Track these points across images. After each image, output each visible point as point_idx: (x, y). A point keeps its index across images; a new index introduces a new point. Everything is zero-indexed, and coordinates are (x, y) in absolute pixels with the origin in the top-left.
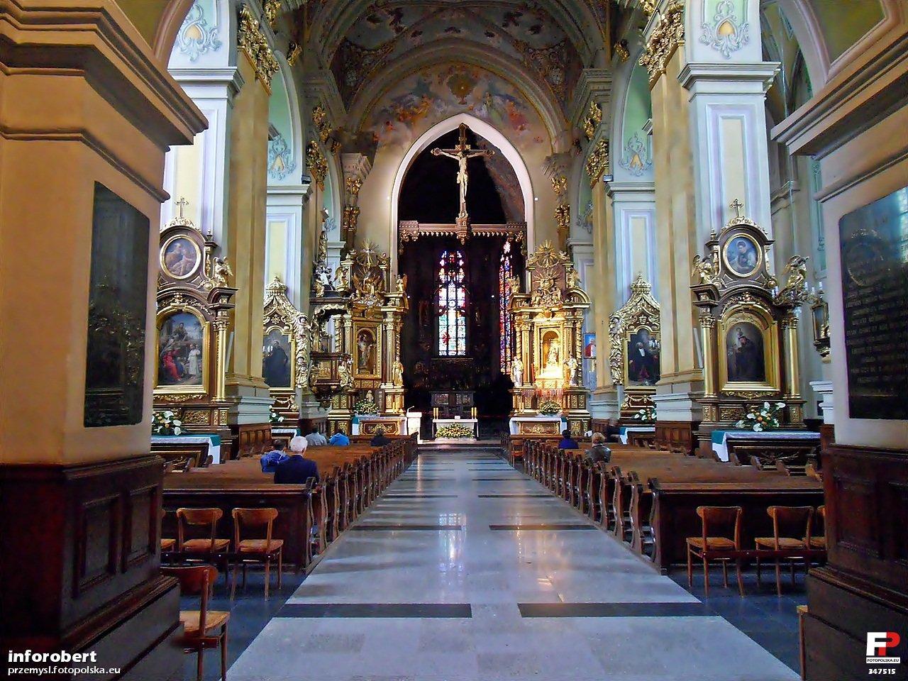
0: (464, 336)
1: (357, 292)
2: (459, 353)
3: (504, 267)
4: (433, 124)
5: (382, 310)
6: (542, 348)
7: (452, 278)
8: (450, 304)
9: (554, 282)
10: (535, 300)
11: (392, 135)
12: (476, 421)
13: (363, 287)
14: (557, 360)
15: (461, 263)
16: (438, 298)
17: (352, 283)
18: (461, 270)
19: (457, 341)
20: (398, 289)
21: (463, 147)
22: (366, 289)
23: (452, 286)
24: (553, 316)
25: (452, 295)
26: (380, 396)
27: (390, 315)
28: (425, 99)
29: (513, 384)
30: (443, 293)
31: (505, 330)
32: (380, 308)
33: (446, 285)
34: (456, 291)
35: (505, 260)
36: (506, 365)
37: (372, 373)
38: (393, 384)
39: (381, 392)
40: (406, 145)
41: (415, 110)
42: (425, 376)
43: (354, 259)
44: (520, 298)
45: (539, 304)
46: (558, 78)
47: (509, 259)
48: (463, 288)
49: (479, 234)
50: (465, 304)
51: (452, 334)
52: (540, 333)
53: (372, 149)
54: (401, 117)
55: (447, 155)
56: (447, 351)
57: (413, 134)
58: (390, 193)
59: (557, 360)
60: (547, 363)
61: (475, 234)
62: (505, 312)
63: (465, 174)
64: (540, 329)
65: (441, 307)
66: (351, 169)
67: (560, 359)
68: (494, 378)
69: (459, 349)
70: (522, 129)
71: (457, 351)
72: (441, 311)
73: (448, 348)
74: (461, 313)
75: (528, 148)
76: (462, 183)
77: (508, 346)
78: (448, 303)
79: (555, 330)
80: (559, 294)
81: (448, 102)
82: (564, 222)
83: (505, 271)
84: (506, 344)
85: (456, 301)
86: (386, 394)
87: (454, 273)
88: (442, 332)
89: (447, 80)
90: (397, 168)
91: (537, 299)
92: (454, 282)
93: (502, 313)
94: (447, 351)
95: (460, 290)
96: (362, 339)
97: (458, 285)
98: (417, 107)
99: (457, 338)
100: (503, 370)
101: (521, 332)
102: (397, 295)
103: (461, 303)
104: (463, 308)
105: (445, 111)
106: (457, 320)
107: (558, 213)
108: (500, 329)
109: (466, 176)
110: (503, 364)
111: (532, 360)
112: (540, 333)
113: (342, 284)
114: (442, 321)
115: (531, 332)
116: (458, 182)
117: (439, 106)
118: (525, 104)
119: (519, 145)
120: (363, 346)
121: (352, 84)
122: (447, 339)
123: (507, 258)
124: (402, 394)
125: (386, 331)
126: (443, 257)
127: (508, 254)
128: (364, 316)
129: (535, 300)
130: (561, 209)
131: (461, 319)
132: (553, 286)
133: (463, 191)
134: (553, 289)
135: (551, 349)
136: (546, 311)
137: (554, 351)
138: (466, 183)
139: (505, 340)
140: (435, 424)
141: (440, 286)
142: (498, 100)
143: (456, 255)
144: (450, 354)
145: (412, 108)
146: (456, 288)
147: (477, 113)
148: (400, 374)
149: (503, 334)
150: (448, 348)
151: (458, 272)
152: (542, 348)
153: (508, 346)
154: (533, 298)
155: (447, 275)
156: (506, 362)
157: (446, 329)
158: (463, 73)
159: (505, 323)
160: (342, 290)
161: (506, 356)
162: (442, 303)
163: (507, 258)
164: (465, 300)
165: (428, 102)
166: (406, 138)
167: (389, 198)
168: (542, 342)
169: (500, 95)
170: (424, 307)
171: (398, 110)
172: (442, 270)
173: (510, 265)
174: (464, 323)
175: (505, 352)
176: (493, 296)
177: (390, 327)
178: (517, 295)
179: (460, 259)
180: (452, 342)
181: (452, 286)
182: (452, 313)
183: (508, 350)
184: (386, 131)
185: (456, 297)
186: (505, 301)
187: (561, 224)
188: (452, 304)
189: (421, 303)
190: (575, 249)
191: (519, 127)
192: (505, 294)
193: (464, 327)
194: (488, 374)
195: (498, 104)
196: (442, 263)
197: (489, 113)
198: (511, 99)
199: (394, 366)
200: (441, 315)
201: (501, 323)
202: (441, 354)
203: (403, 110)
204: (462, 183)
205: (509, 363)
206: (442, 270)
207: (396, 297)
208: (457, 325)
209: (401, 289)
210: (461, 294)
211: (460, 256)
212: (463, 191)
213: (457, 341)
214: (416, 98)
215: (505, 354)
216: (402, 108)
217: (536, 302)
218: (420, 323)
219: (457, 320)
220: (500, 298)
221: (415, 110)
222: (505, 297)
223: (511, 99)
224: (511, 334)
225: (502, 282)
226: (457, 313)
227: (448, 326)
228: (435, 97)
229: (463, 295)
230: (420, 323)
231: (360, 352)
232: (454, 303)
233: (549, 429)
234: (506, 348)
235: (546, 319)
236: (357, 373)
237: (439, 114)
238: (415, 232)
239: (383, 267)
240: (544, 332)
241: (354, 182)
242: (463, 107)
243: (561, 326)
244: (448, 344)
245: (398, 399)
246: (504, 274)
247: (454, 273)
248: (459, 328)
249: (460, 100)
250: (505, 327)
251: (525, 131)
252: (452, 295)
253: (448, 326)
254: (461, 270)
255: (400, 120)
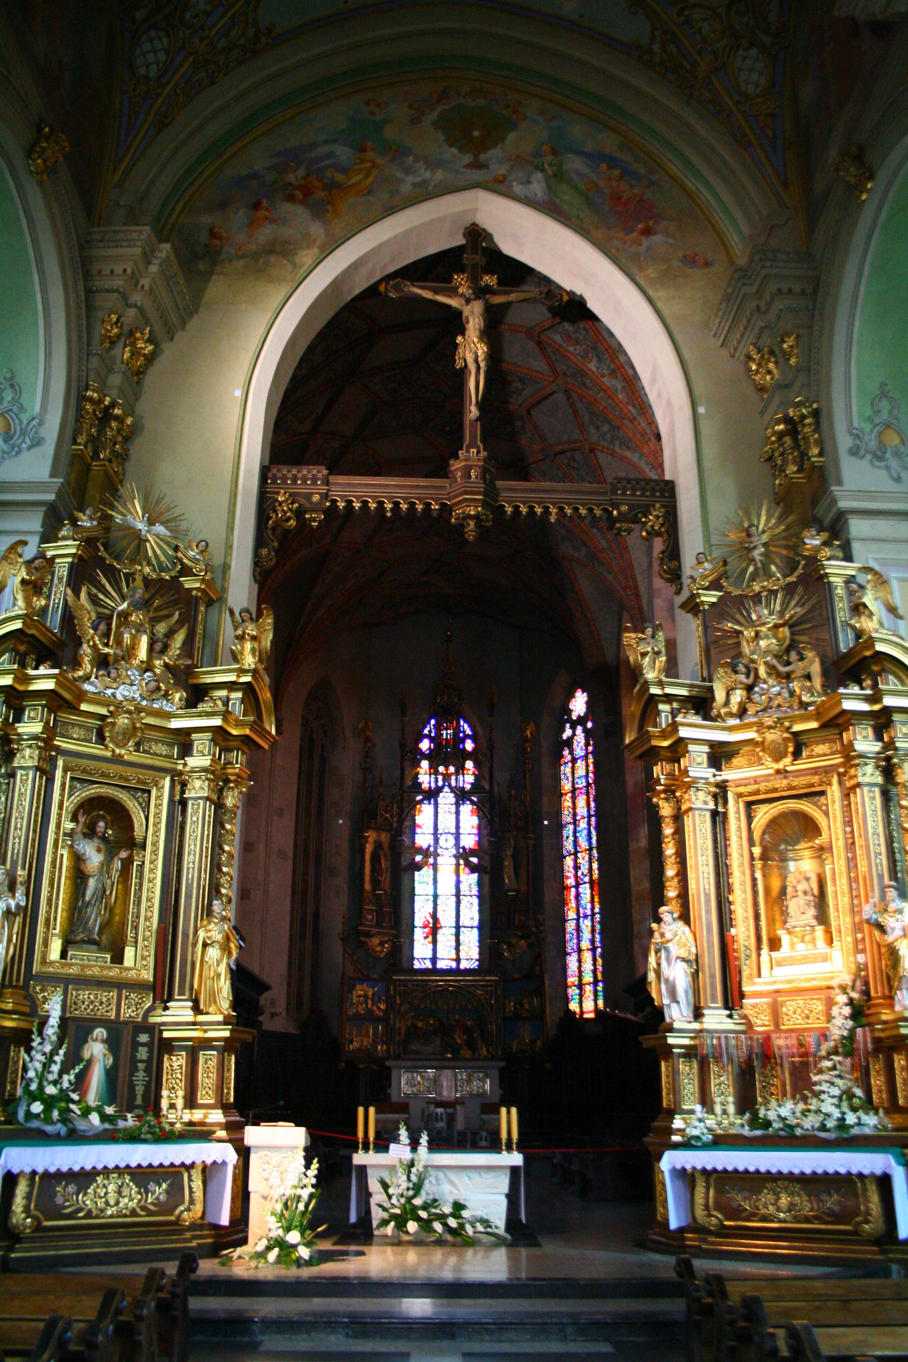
0: (476, 923)
1: (86, 649)
2: (464, 965)
3: (571, 753)
4: (388, 211)
5: (175, 724)
6: (758, 875)
7: (447, 777)
8: (442, 842)
9: (792, 634)
10: (727, 703)
11: (264, 234)
12: (516, 1159)
13: (107, 635)
14: (822, 918)
15: (469, 745)
16: (414, 826)
17: (69, 618)
18: (469, 764)
19: (457, 935)
20: (235, 657)
21: (474, 280)
22: (119, 642)
23: (447, 799)
24: (797, 755)
25: (447, 822)
26: (143, 1053)
27: (201, 742)
28: (370, 155)
29: (658, 1013)
30: (424, 815)
31: (578, 905)
32: (169, 716)
33: (432, 795)
34: (458, 813)
35: (574, 734)
36: (581, 996)
37: (118, 958)
38: (197, 1010)
39: (144, 1038)
40: (306, 257)
41: (339, 177)
42: (375, 1020)
43: (89, 543)
44: (669, 698)
45: (742, 712)
46: (754, 77)
47: (586, 731)
48: (472, 803)
49: (524, 510)
50: (479, 843)
51: (447, 917)
52: (750, 819)
53: (201, 266)
54: (298, 193)
55: (427, 294)
56: (434, 960)
57: (326, 230)
58: (242, 378)
59: (822, 918)
60: (781, 933)
61: (509, 510)
62: (576, 858)
63: (481, 339)
64: (749, 805)
65: (420, 850)
66: (118, 283)
67: (840, 918)
68: (552, 1032)
69: (462, 955)
70: (647, 232)
71: (458, 960)
72: (418, 858)
73: (435, 951)
74: (468, 864)
75: (667, 277)
76: (472, 367)
77: (585, 944)
78: (436, 840)
79: (804, 806)
80: (816, 668)
81: (433, 164)
82: (804, 455)
83: (574, 760)
84: (579, 939)
85: (457, 836)
86: (168, 1047)
87: (452, 769)
88: (422, 911)
89: (434, 116)
90: (269, 315)
91: (738, 696)
92: (452, 790)
93: (569, 862)
94: (434, 960)
95: (466, 809)
96: (90, 833)
97: (461, 796)
98: (345, 171)
99: (458, 927)
100: (574, 1006)
101: (678, 818)
102: (232, 678)
103: (469, 841)
104: (472, 852)
105: (425, 183)
106: (458, 882)
107: (781, 435)
108: (564, 903)
109: (482, 350)
110: (573, 992)
111: (725, 919)
112: (750, 819)
113: (21, 603)
114: (422, 880)
115: (718, 818)
116: (459, 364)
117: (408, 171)
118: (656, 177)
119: (641, 269)
120: (94, 857)
121: (153, 71)
122: (434, 929)
123: (579, 729)
124: (228, 1046)
125: (183, 803)
126: (426, 731)
127: (581, 721)
128: (101, 739)
129: (727, 703)
130: (787, 420)
131: (470, 881)
132: (788, 651)
133: (474, 385)
134: (793, 656)
135: (791, 880)
136: (771, 736)
137: (802, 887)
138: (482, 365)
139: (578, 929)
140: (363, 1169)
141: (419, 798)
142: (574, 164)
143: (457, 730)
144: (440, 965)
145: (328, 174)
146: (457, 805)
147: (518, 189)
148: (223, 969)
149: (572, 915)
150: (435, 951)
151: (461, 769)
152: (758, 875)
153: (585, 944)
154: (720, 695)
155: (436, 773)
156: (580, 986)
157: (431, 905)
158: (481, 102)
159: (577, 885)
160: (18, 625)
161: (580, 972)
162: (423, 839)
163: (579, 729)
164: (479, 834)
165: (379, 161)
166: (308, 241)
167: (238, 393)
168: (757, 851)
169: (580, 153)
170: (378, 846)
171: (291, 178)
172: (425, 764)
173: (587, 744)
174: (475, 891)
175: (580, 961)
176: (546, 823)
177: (198, 788)
178: (661, 684)
179: (468, 737)
180: (446, 937)
181: (447, 799)
182: (447, 861)
183: (587, 956)
184: (252, 224)
185: (458, 827)
186: (575, 832)
187: (792, 469)
188: (447, 843)
189: (371, 836)
190: (857, 527)
191: (640, 226)
192: (575, 815)
193: (475, 901)
194: (539, 1016)
195: (577, 172)
196: (425, 745)
197: (550, 189)
198: (612, 162)
199: (202, 934)
200: (419, 867)
201: (567, 888)
202: (417, 965)
203: (303, 178)
204: (472, 367)
205: (589, 989)
206: (425, 764)
207: (231, 686)
208: (458, 895)
209: (249, 661)
210: (470, 820)
211: (469, 732)
212: (474, 385)
213: (457, 935)
214: (343, 153)
215: (580, 967)
216: (301, 172)
217: (734, 709)
218: (368, 886)
219: (458, 882)
220: (561, 826)
221: (339, 177)
222: (575, 823)
223: (612, 162)
224: (593, 914)
225: (567, 786)
226: (458, 865)
227: (436, 897)
228: (398, 152)
229: (475, 821)
230: (368, 886)
231: (79, 876)
232: (452, 840)
233: (831, 1201)
234: (580, 951)
235: (769, 767)
236: (54, 954)
237: (406, 188)
238: (316, 498)
239: (189, 583)
240: (764, 814)
241: (131, 334)
242: (478, 175)
243: (834, 791)
244: (434, 942)
245: (208, 1061)
246: (573, 768)
247: (452, 769)
248: (464, 901)
249: (468, 159)
250: (578, 896)
251: (657, 239)
252: (447, 822)
253: (436, 897)
254: (469, 764)
255: (291, 198)
